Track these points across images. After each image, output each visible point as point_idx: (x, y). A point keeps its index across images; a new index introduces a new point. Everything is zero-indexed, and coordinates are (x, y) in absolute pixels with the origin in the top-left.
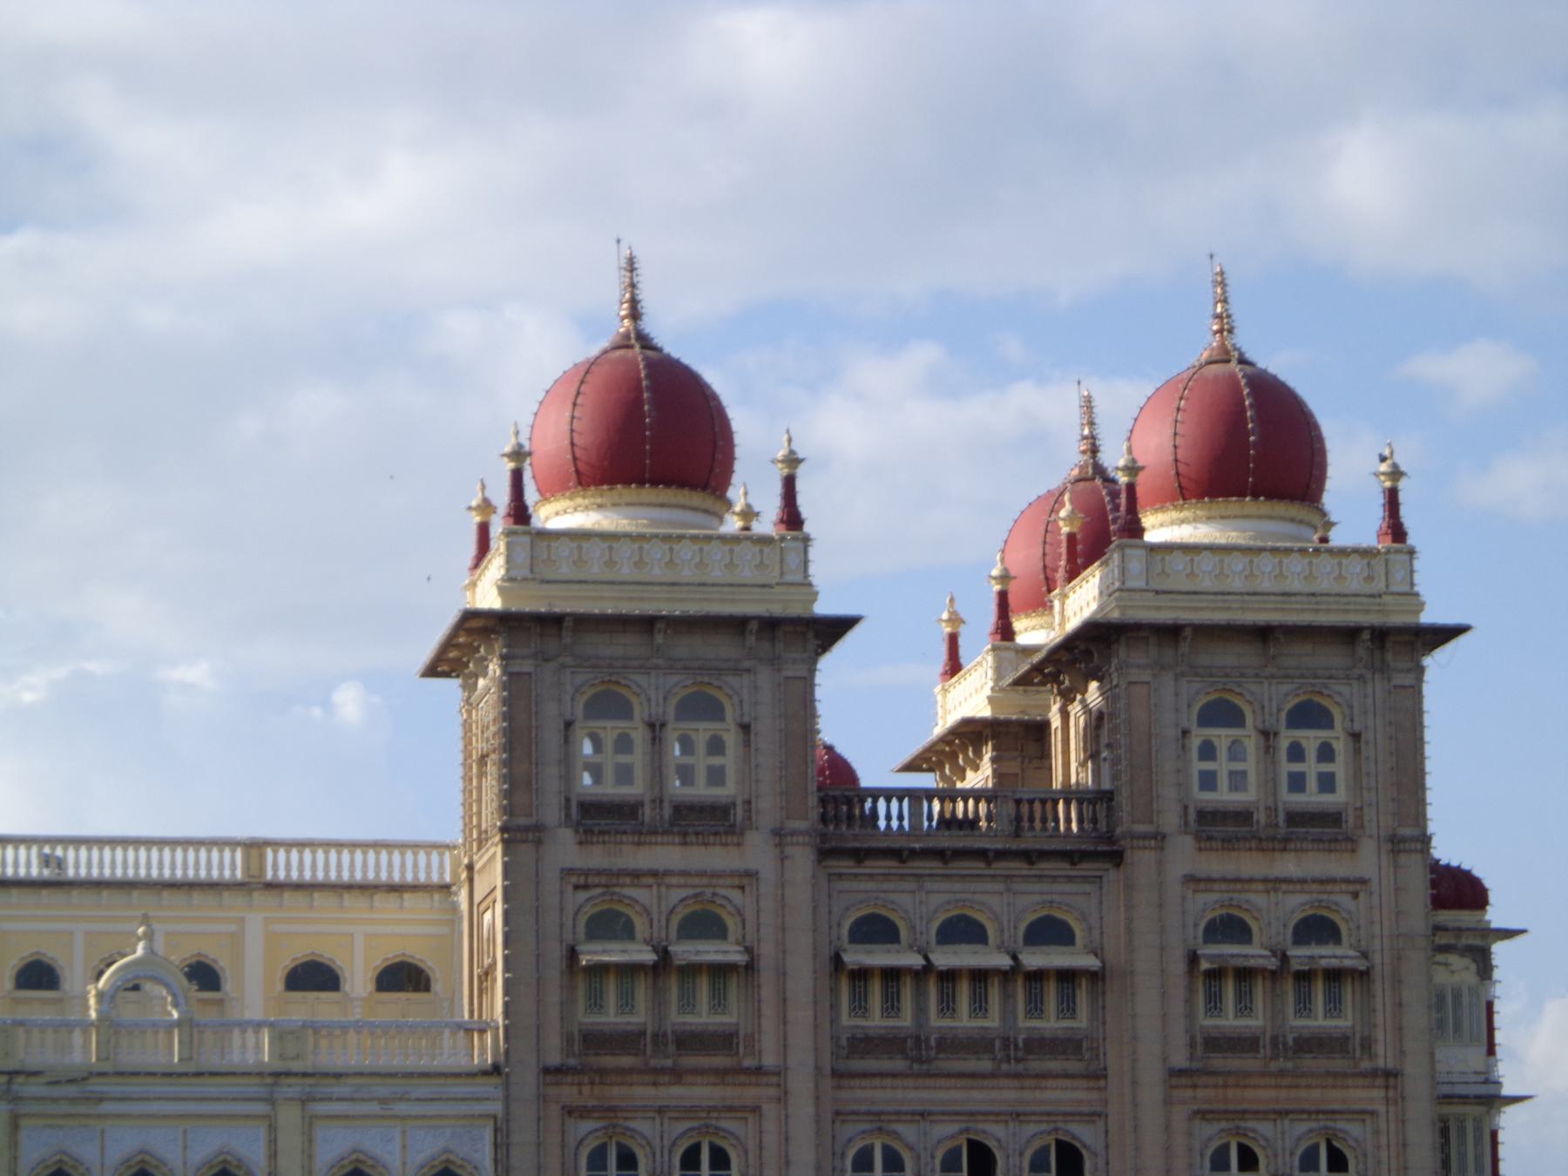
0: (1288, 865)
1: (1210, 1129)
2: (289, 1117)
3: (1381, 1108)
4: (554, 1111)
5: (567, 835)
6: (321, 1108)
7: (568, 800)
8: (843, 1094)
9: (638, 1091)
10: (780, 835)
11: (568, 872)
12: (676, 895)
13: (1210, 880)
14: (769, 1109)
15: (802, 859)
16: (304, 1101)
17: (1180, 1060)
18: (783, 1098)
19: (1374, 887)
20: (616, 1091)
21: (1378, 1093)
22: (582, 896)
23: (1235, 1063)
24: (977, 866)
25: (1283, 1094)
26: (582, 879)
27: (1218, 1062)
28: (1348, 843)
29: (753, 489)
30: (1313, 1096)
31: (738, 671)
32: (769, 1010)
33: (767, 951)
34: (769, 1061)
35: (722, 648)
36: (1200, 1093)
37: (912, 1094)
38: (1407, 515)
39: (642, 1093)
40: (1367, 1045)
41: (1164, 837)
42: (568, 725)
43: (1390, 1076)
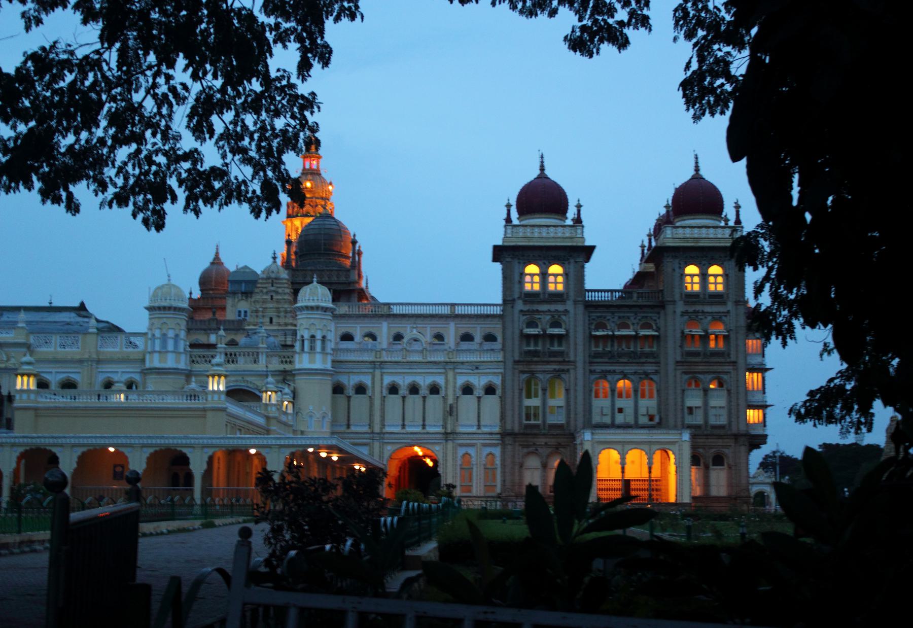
1: (686, 377)
2: (450, 374)
4: (517, 371)
10: (576, 302)
11: (521, 311)
14: (572, 371)
15: (581, 308)
16: (454, 369)
17: (679, 359)
18: (575, 369)
22: (525, 317)
23: (694, 359)
28: (724, 303)
29: (571, 213)
30: (715, 368)
32: (572, 347)
34: (572, 359)
38: (742, 218)
39: (539, 367)
40: (729, 355)
41: (674, 302)
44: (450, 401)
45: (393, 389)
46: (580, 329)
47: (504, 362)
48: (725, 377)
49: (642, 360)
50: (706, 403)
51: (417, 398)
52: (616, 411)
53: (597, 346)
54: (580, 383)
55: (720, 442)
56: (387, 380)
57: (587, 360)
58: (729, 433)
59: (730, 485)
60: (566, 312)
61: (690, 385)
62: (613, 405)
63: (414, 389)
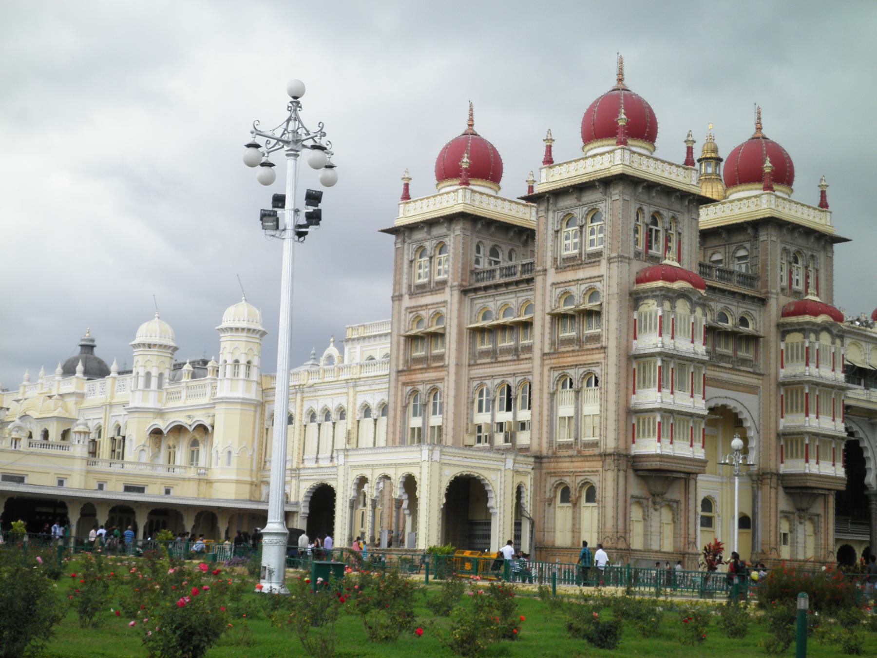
0: (581, 274)
1: (556, 374)
2: (351, 391)
3: (603, 361)
5: (406, 297)
6: (358, 389)
8: (472, 372)
11: (407, 308)
12: (431, 311)
13: (558, 283)
14: (446, 378)
15: (456, 294)
16: (355, 386)
17: (547, 350)
18: (448, 375)
19: (605, 278)
20: (413, 377)
21: (602, 355)
22: (411, 315)
24: (503, 290)
25: (575, 358)
27: (563, 349)
31: (446, 236)
32: (447, 346)
33: (448, 327)
34: (447, 363)
36: (552, 361)
39: (419, 377)
41: (545, 270)
42: (411, 262)
43: (605, 348)
44: (349, 428)
45: (313, 417)
46: (455, 322)
47: (389, 374)
48: (597, 370)
49: (522, 356)
50: (578, 410)
51: (330, 423)
54: (452, 393)
55: (587, 466)
56: (306, 407)
57: (465, 361)
58: (596, 451)
59: (601, 531)
60: (445, 302)
61: (564, 386)
63: (327, 415)
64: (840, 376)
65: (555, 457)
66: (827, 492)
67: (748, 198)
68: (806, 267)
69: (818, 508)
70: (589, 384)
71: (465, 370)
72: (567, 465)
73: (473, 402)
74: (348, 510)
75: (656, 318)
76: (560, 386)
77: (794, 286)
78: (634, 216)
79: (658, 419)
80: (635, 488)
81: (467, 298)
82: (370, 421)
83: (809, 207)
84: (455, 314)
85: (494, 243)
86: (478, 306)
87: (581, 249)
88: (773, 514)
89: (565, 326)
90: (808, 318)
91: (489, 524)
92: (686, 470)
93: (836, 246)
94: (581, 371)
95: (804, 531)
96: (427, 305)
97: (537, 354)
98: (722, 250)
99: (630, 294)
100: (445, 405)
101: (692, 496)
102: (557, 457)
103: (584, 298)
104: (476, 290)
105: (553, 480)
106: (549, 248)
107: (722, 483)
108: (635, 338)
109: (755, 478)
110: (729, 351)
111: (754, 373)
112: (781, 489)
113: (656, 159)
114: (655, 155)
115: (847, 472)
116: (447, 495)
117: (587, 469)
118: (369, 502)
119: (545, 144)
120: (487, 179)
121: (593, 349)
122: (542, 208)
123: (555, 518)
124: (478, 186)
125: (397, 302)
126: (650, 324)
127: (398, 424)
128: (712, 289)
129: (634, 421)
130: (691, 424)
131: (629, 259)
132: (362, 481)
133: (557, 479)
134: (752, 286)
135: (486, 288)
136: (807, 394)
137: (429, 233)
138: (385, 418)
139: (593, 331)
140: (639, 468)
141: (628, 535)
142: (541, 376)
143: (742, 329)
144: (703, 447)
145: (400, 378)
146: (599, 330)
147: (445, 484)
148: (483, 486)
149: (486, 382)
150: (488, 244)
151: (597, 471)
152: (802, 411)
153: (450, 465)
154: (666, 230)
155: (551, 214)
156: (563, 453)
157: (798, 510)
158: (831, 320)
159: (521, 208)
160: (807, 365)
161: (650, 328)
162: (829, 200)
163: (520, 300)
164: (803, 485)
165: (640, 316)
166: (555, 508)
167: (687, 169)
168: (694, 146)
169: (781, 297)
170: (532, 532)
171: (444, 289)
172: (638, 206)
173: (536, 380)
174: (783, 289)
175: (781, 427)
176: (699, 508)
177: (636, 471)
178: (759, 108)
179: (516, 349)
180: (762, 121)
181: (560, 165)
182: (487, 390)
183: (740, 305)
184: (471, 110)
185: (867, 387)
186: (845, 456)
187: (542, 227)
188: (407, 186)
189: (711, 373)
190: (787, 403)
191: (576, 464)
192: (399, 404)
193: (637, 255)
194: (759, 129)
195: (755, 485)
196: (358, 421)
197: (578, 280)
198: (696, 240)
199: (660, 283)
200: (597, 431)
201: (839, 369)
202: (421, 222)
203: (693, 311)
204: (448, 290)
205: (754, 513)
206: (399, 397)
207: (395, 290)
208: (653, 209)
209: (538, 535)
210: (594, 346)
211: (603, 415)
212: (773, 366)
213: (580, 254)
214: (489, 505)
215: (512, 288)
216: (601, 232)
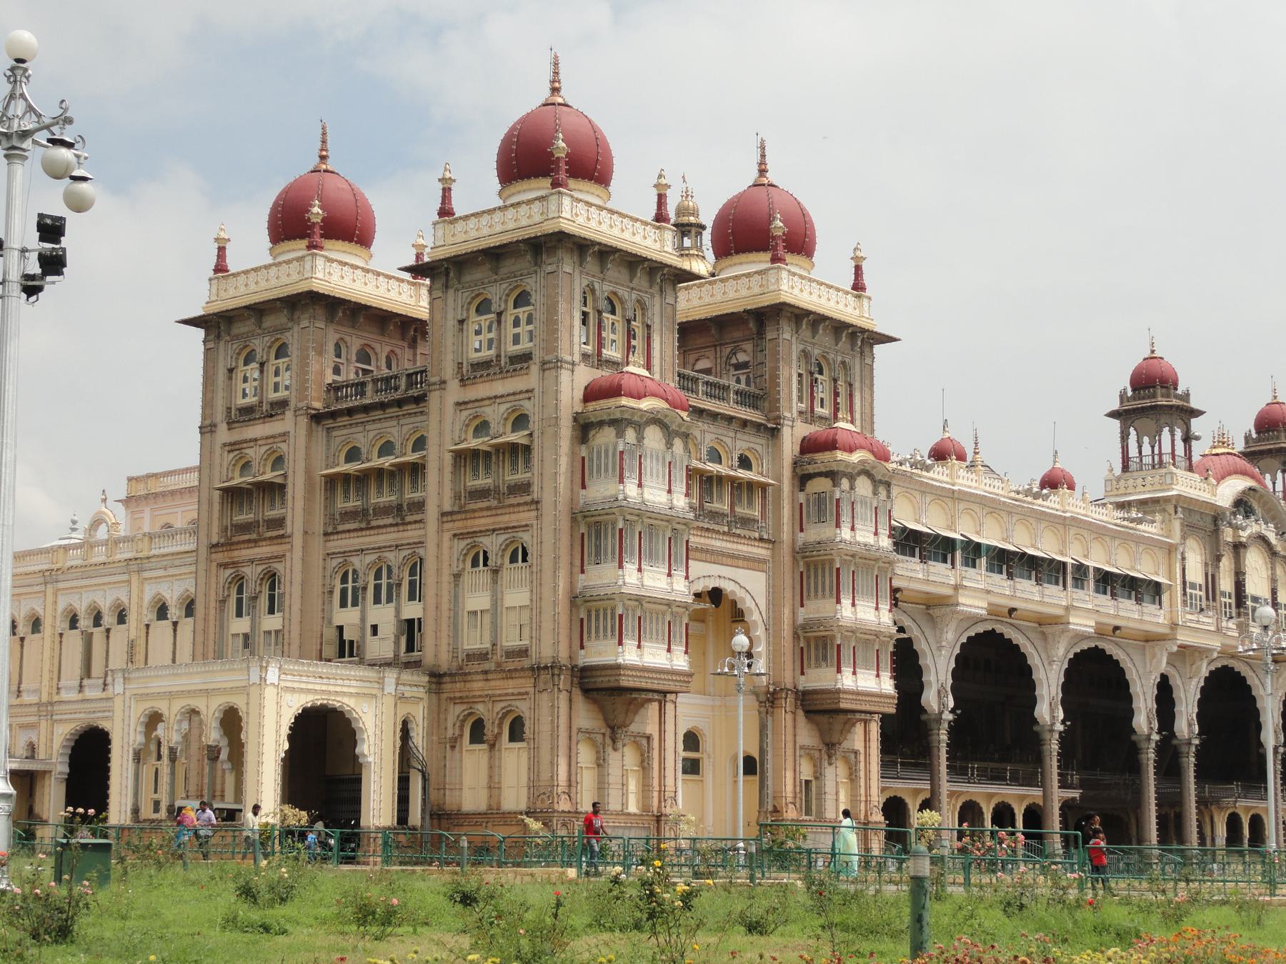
0: (499, 387)
1: (463, 543)
5: (224, 426)
6: (146, 574)
7: (229, 409)
8: (330, 544)
9: (244, 552)
11: (225, 445)
13: (465, 403)
14: (288, 558)
15: (304, 421)
17: (447, 507)
18: (291, 550)
19: (536, 391)
20: (236, 553)
21: (534, 514)
22: (232, 455)
24: (377, 414)
26: (233, 446)
27: (473, 506)
33: (290, 474)
35: (281, 319)
37: (356, 541)
41: (444, 382)
42: (231, 371)
43: (537, 502)
44: (132, 637)
46: (301, 466)
48: (525, 537)
50: (496, 601)
52: (369, 631)
53: (347, 497)
54: (297, 578)
55: (512, 686)
57: (318, 526)
58: (526, 663)
59: (532, 785)
60: (284, 434)
62: (363, 619)
64: (885, 542)
65: (459, 674)
66: (868, 717)
67: (748, 275)
68: (835, 381)
69: (856, 739)
70: (513, 559)
71: (318, 544)
72: (480, 684)
73: (331, 592)
74: (131, 766)
75: (614, 455)
76: (469, 563)
77: (818, 410)
78: (578, 297)
79: (620, 611)
80: (585, 717)
81: (320, 429)
82: (166, 625)
83: (838, 290)
84: (301, 454)
85: (363, 342)
86: (338, 440)
87: (499, 348)
88: (790, 752)
89: (475, 470)
90: (840, 455)
91: (359, 781)
92: (661, 687)
93: (878, 349)
94: (502, 538)
95: (835, 775)
96: (256, 440)
97: (432, 513)
98: (710, 353)
99: (575, 419)
100: (287, 596)
101: (669, 727)
102: (466, 674)
103: (504, 425)
104: (333, 415)
105: (459, 709)
106: (450, 348)
107: (713, 707)
108: (584, 487)
109: (763, 698)
110: (726, 508)
111: (761, 540)
112: (800, 713)
113: (612, 212)
114: (609, 205)
115: (896, 687)
116: (290, 738)
117: (510, 691)
118: (165, 752)
119: (440, 186)
120: (351, 241)
121: (519, 505)
122: (439, 284)
123: (461, 767)
124: (336, 250)
125: (208, 435)
126: (606, 465)
127: (212, 630)
128: (699, 413)
129: (583, 615)
130: (668, 618)
131: (573, 364)
132: (154, 719)
133: (465, 707)
134: (755, 407)
135: (350, 412)
136: (838, 570)
137: (259, 323)
138: (190, 620)
139: (521, 476)
140: (591, 686)
141: (573, 790)
142: (439, 548)
143: (742, 474)
144: (686, 652)
145: (214, 556)
146: (529, 475)
147: (288, 719)
148: (348, 722)
149: (352, 559)
150: (355, 343)
151: (527, 693)
152: (831, 596)
153: (293, 690)
154: (629, 321)
155: (451, 292)
156: (475, 667)
157: (827, 745)
158: (872, 457)
159: (405, 286)
160: (838, 525)
161: (606, 470)
162: (867, 279)
163: (405, 429)
164: (834, 706)
165: (591, 452)
166: (461, 752)
167: (658, 228)
168: (668, 192)
169: (799, 424)
170: (424, 789)
171: (283, 413)
172: (585, 283)
173: (429, 553)
174: (801, 413)
175: (800, 621)
176: (681, 746)
177: (587, 691)
178: (763, 141)
179: (399, 508)
180: (768, 160)
181: (466, 218)
182: (355, 571)
183: (739, 435)
184: (324, 134)
185: (923, 559)
186: (893, 662)
187: (438, 316)
188: (221, 251)
189: (695, 540)
190: (809, 584)
191: (493, 683)
192: (213, 597)
193: (585, 356)
194: (762, 172)
195: (763, 709)
196: (148, 626)
197: (496, 397)
198: (672, 339)
199: (625, 401)
200: (526, 631)
201: (884, 532)
202: (247, 307)
203: (669, 445)
204: (289, 414)
205: (762, 752)
206: (214, 586)
207: (204, 417)
208: (608, 288)
209: (434, 795)
210: (521, 500)
211: (535, 607)
212: (786, 528)
213: (498, 356)
214: (357, 751)
215: (393, 411)
216: (529, 321)
